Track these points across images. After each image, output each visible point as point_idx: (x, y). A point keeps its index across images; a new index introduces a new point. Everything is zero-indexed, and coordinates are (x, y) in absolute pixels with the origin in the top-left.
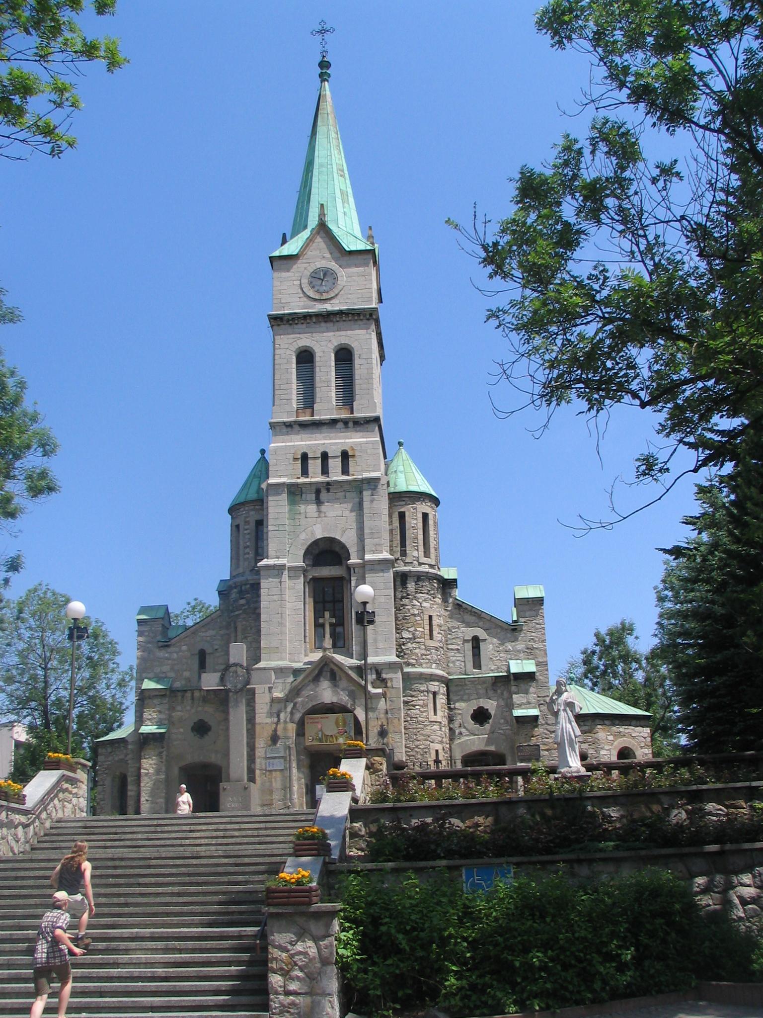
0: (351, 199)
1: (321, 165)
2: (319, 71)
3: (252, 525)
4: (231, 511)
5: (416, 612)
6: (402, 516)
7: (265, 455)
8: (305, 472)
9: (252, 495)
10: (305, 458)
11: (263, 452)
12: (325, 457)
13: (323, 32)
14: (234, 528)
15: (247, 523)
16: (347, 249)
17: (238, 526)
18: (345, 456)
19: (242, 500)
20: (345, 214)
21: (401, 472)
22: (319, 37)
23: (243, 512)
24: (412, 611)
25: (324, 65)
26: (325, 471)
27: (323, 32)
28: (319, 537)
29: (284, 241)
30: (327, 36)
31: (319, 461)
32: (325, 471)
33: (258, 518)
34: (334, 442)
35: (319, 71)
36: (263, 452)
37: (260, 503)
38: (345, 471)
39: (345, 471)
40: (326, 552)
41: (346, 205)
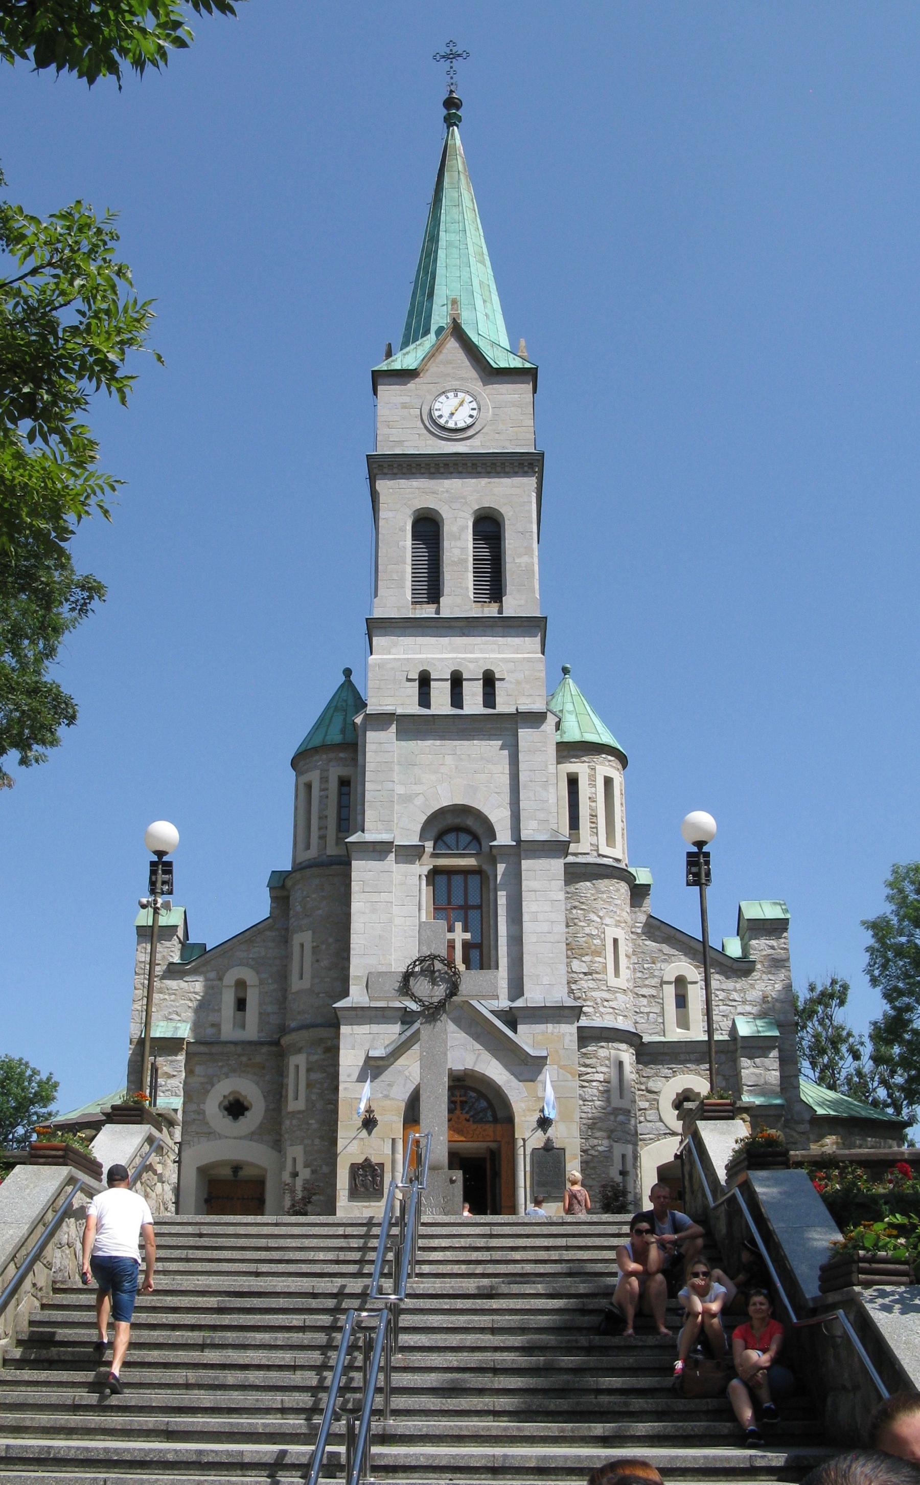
0: (495, 298)
1: (450, 244)
2: (445, 112)
3: (333, 785)
4: (294, 763)
5: (595, 932)
6: (573, 782)
7: (353, 678)
8: (425, 699)
9: (335, 736)
10: (425, 681)
11: (348, 672)
12: (457, 681)
13: (451, 56)
14: (302, 788)
15: (324, 779)
16: (495, 366)
17: (309, 786)
18: (489, 681)
19: (317, 741)
20: (486, 315)
21: (569, 712)
22: (446, 65)
23: (319, 760)
24: (587, 930)
25: (451, 103)
26: (457, 699)
27: (451, 56)
28: (445, 804)
29: (389, 354)
30: (458, 63)
31: (448, 684)
32: (457, 699)
33: (344, 771)
34: (474, 654)
35: (445, 112)
36: (348, 672)
37: (351, 748)
38: (489, 698)
39: (489, 698)
40: (456, 826)
41: (488, 304)
